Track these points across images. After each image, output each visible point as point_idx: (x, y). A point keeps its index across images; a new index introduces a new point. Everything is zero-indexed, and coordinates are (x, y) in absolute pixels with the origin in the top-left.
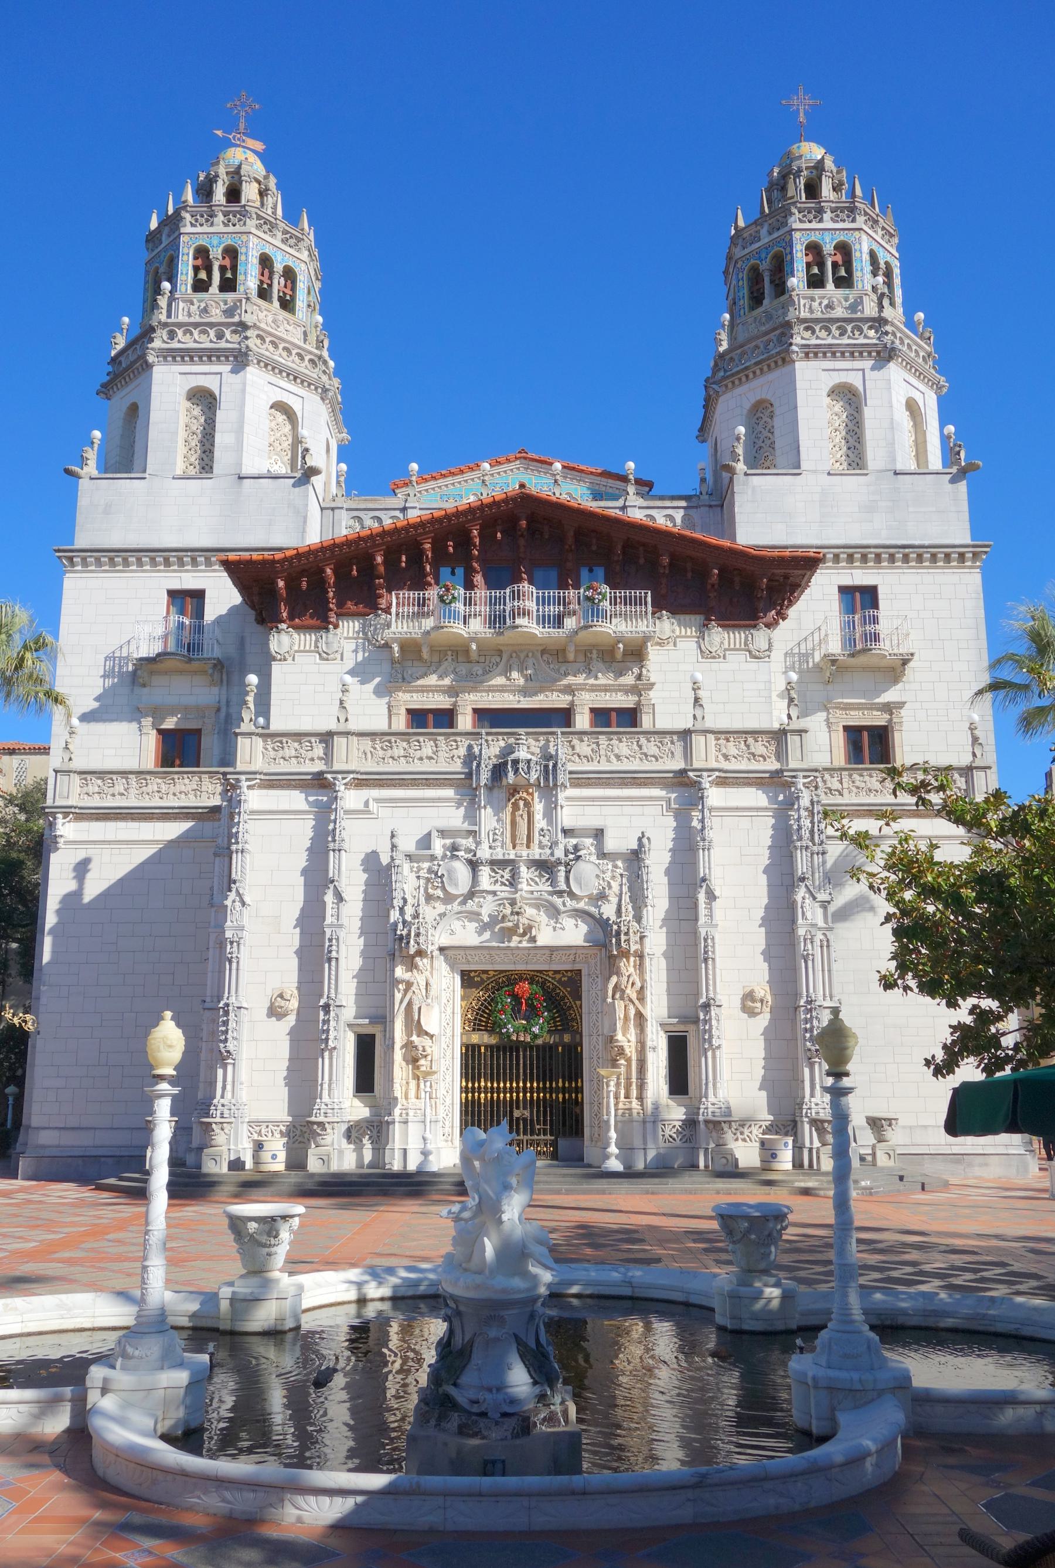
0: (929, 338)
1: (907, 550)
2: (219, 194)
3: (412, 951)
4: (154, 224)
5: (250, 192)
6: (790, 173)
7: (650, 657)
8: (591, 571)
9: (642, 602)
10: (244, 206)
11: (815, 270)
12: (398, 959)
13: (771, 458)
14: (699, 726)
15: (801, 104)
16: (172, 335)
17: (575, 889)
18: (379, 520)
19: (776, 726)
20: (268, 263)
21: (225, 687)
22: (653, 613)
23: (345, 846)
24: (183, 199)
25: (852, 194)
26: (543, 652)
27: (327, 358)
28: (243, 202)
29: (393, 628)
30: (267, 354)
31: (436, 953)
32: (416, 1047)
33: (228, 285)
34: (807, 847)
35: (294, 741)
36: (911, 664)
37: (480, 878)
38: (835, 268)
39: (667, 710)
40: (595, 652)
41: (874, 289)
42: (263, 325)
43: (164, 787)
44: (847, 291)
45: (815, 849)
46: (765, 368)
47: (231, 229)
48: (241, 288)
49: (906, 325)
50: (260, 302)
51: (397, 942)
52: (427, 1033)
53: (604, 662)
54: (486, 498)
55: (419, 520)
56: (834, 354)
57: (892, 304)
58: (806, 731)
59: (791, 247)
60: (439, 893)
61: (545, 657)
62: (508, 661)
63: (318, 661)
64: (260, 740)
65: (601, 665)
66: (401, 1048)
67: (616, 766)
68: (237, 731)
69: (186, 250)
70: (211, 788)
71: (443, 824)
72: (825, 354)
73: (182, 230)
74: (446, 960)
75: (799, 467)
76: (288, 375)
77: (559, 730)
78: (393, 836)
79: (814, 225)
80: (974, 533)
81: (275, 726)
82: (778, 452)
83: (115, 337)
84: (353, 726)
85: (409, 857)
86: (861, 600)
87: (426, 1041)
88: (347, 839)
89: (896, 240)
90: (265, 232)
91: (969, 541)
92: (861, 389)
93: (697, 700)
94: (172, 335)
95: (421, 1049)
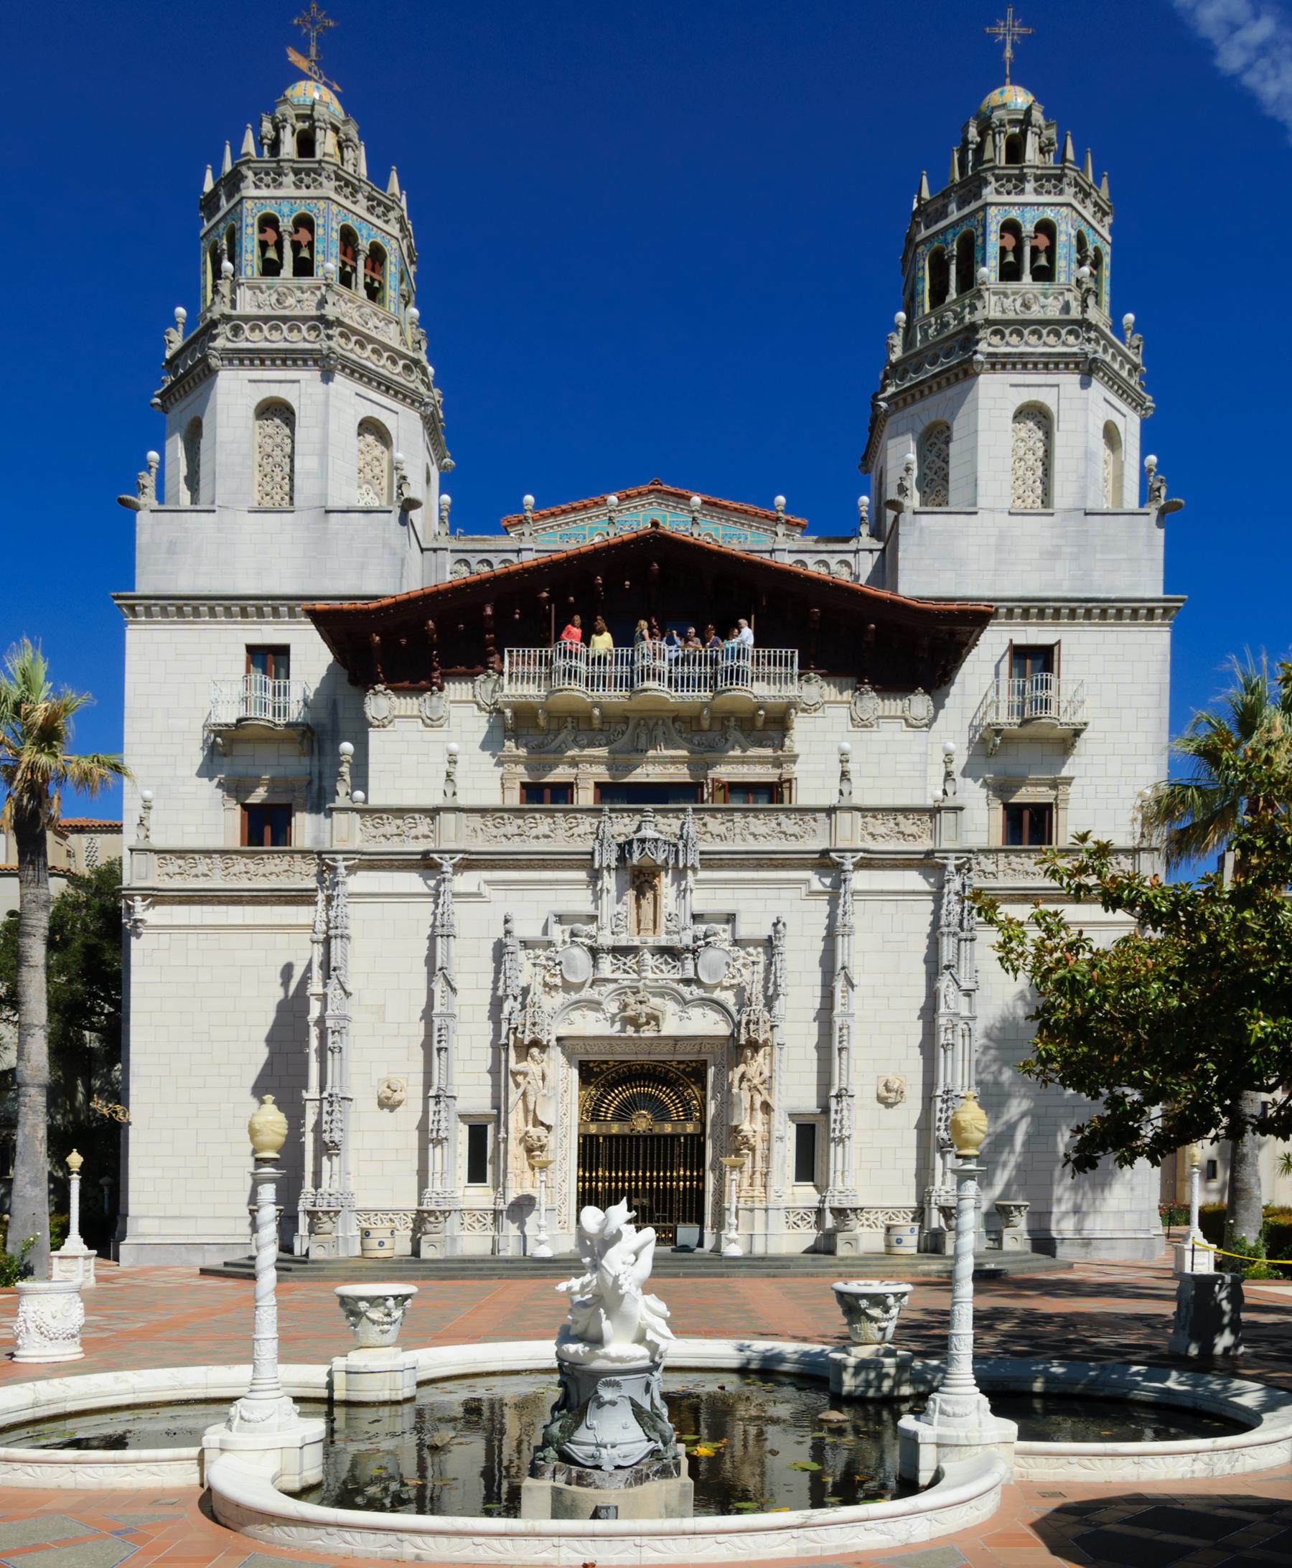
0: (1138, 347)
2: (289, 146)
4: (208, 185)
5: (326, 144)
6: (989, 127)
7: (795, 725)
9: (787, 662)
10: (320, 162)
11: (1010, 258)
13: (943, 493)
15: (1009, 32)
18: (489, 563)
20: (351, 239)
21: (316, 758)
22: (800, 676)
24: (244, 151)
25: (1061, 157)
26: (675, 719)
28: (318, 156)
29: (506, 691)
33: (304, 268)
35: (396, 818)
37: (601, 966)
40: (733, 719)
42: (346, 320)
44: (1046, 285)
47: (304, 192)
48: (319, 272)
49: (1113, 329)
50: (343, 289)
53: (742, 730)
54: (613, 540)
55: (535, 563)
56: (1025, 365)
57: (1098, 303)
59: (984, 227)
61: (677, 725)
62: (635, 728)
63: (421, 727)
64: (358, 816)
65: (738, 735)
68: (332, 805)
69: (250, 221)
71: (561, 908)
73: (245, 193)
75: (975, 504)
76: (379, 384)
77: (690, 807)
81: (375, 800)
82: (952, 485)
83: (168, 334)
90: (347, 198)
92: (1054, 409)
94: (236, 330)
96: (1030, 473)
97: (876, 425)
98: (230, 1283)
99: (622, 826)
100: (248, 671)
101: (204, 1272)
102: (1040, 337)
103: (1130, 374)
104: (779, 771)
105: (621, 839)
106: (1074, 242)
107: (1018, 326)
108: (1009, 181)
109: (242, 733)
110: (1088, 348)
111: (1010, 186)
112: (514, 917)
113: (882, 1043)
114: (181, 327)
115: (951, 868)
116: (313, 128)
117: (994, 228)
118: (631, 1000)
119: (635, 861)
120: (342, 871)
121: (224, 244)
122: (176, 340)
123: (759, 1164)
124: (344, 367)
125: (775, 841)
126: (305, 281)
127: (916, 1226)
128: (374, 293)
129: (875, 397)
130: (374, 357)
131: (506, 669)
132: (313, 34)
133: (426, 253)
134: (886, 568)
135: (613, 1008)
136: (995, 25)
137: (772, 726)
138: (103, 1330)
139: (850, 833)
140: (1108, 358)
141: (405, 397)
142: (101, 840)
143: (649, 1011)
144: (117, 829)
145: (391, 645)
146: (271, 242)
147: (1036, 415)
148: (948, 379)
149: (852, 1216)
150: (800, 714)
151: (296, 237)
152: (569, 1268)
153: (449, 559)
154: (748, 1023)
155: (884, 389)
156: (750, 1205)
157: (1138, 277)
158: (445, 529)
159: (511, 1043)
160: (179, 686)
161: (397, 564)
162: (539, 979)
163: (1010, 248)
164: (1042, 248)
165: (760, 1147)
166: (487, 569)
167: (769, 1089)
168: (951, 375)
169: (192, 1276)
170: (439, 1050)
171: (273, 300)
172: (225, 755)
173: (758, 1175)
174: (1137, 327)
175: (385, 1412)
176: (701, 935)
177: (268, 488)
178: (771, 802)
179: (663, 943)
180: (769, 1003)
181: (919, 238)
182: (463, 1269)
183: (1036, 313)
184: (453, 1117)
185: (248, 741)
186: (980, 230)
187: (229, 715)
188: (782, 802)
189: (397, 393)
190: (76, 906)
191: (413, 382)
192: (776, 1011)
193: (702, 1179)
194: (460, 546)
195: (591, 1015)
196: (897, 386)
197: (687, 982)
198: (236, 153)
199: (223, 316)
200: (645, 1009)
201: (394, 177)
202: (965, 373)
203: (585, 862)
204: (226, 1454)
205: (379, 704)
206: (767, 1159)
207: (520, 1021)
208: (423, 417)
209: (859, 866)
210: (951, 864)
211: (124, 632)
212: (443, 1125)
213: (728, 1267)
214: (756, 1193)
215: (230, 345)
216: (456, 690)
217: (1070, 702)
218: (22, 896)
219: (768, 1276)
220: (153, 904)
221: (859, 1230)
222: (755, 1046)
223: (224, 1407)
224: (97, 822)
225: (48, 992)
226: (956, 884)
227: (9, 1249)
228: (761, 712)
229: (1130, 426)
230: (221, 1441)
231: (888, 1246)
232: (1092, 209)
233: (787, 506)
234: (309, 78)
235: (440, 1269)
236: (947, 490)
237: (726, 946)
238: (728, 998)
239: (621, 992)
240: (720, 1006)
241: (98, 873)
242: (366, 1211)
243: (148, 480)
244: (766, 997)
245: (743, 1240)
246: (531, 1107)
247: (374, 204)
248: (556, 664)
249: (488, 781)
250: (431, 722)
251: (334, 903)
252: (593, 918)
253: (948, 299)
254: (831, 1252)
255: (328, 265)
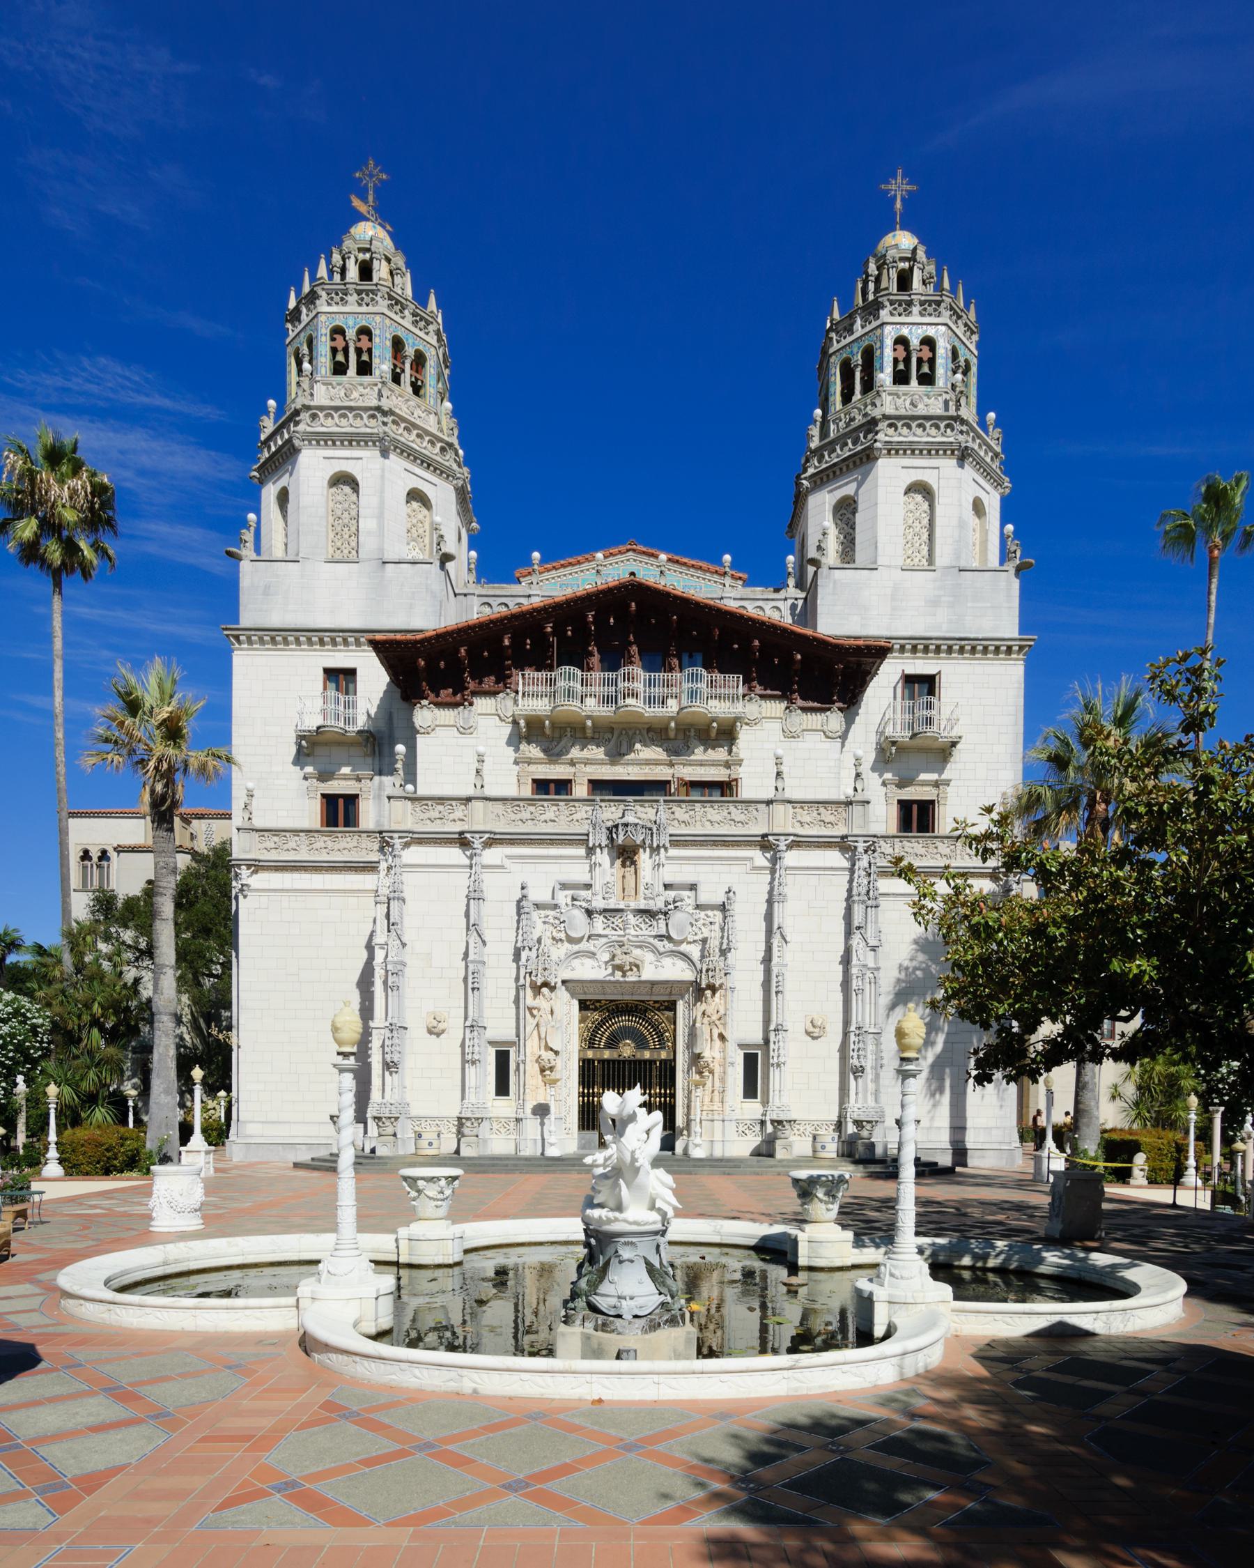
1: (963, 643)
2: (353, 273)
4: (292, 304)
5: (381, 271)
6: (884, 263)
7: (740, 736)
8: (691, 656)
10: (376, 285)
11: (901, 366)
14: (779, 797)
15: (899, 188)
16: (314, 416)
17: (674, 935)
18: (506, 605)
19: (842, 798)
22: (744, 696)
23: (485, 895)
25: (939, 287)
26: (649, 730)
27: (457, 446)
28: (375, 280)
30: (402, 439)
33: (365, 369)
34: (864, 902)
36: (958, 746)
38: (916, 367)
39: (753, 784)
41: (953, 386)
42: (397, 411)
43: (330, 844)
44: (929, 388)
45: (869, 903)
46: (851, 466)
47: (364, 309)
48: (376, 372)
50: (394, 386)
56: (913, 451)
58: (868, 802)
59: (882, 342)
60: (562, 936)
67: (709, 830)
69: (324, 331)
70: (369, 845)
72: (905, 451)
75: (875, 562)
76: (422, 462)
77: (662, 799)
78: (523, 888)
79: (903, 319)
80: (1023, 628)
81: (422, 792)
84: (488, 792)
85: (538, 906)
86: (922, 686)
88: (485, 889)
89: (975, 338)
91: (1016, 635)
92: (935, 487)
93: (779, 774)
96: (916, 538)
97: (799, 500)
98: (316, 1174)
99: (610, 812)
100: (325, 688)
101: (297, 1165)
102: (924, 430)
103: (992, 459)
104: (728, 772)
105: (610, 824)
106: (950, 354)
107: (908, 420)
108: (900, 305)
109: (321, 738)
110: (961, 438)
111: (901, 309)
112: (529, 885)
113: (811, 990)
114: (272, 415)
115: (860, 849)
116: (372, 259)
117: (889, 342)
118: (618, 951)
119: (620, 842)
120: (398, 846)
121: (305, 350)
122: (268, 425)
123: (717, 1084)
124: (396, 447)
125: (727, 827)
126: (366, 379)
127: (836, 1135)
128: (417, 389)
129: (798, 477)
130: (418, 440)
131: (520, 688)
132: (371, 185)
133: (456, 359)
134: (807, 612)
135: (606, 957)
136: (888, 183)
137: (726, 734)
138: (220, 1208)
139: (783, 821)
140: (976, 447)
141: (442, 472)
142: (216, 824)
143: (632, 960)
144: (228, 817)
145: (432, 668)
146: (340, 348)
147: (921, 489)
148: (854, 463)
149: (787, 1126)
150: (745, 727)
151: (359, 345)
152: (574, 1165)
153: (476, 602)
154: (707, 971)
155: (805, 470)
156: (710, 1117)
157: (999, 384)
158: (472, 578)
159: (528, 985)
160: (274, 699)
161: (433, 603)
162: (549, 934)
163: (901, 359)
164: (925, 359)
165: (717, 1070)
166: (504, 609)
167: (724, 1025)
168: (857, 459)
169: (288, 1169)
170: (473, 989)
171: (342, 394)
172: (308, 755)
173: (716, 1093)
174: (997, 424)
175: (439, 1273)
176: (671, 900)
177: (339, 544)
178: (722, 795)
179: (642, 907)
180: (724, 953)
181: (831, 351)
182: (493, 1165)
183: (921, 410)
184: (484, 1043)
185: (326, 744)
186: (878, 345)
187: (312, 722)
188: (732, 795)
189: (436, 469)
190: (197, 875)
191: (449, 461)
192: (729, 961)
193: (673, 1096)
194: (484, 593)
195: (589, 962)
196: (816, 467)
197: (660, 937)
198: (313, 278)
199: (304, 406)
200: (628, 959)
201: (432, 299)
202: (866, 458)
203: (582, 840)
204: (317, 1302)
205: (424, 715)
206: (723, 1080)
207: (534, 967)
208: (456, 489)
209: (790, 847)
210: (861, 847)
211: (231, 658)
212: (477, 1049)
213: (695, 1166)
214: (715, 1108)
215: (309, 429)
216: (483, 704)
217: (949, 720)
218: (156, 864)
219: (724, 1173)
220: (255, 872)
221: (792, 1138)
222: (713, 989)
223: (311, 1268)
224: (213, 811)
225: (177, 944)
226: (864, 863)
227: (148, 1145)
228: (715, 724)
229: (993, 502)
230: (312, 1292)
231: (814, 1151)
232: (963, 328)
233: (732, 563)
234: (368, 220)
235: (475, 1165)
236: (854, 550)
237: (690, 909)
238: (694, 951)
239: (611, 944)
240: (686, 957)
241: (214, 850)
242: (419, 1118)
243: (248, 536)
244: (721, 950)
245: (706, 1146)
246: (543, 1036)
247: (418, 319)
248: (558, 684)
249: (507, 773)
250: (465, 730)
251: (392, 872)
252: (588, 886)
253: (854, 399)
254: (771, 1155)
255: (383, 366)
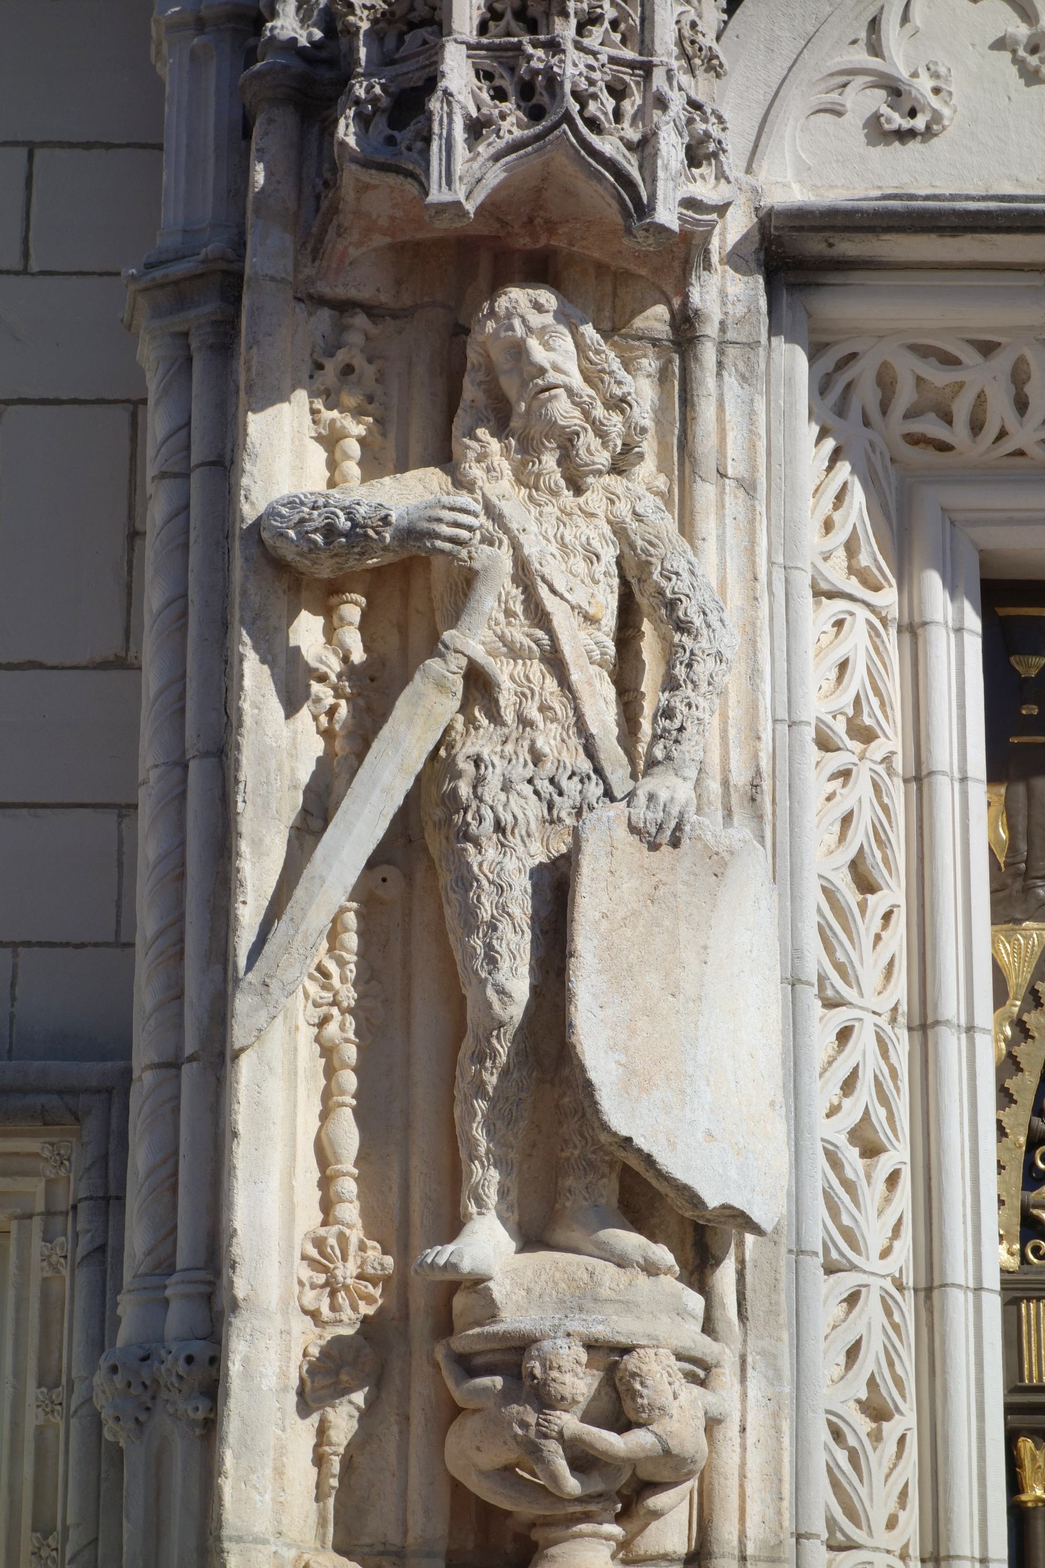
3: (465, 175)
12: (272, 325)
31: (726, 293)
32: (515, 1359)
51: (274, 132)
52: (645, 1195)
66: (323, 1379)
74: (834, 396)
87: (638, 1295)
95: (579, 1383)
